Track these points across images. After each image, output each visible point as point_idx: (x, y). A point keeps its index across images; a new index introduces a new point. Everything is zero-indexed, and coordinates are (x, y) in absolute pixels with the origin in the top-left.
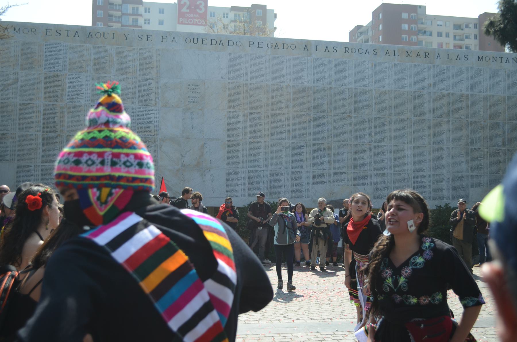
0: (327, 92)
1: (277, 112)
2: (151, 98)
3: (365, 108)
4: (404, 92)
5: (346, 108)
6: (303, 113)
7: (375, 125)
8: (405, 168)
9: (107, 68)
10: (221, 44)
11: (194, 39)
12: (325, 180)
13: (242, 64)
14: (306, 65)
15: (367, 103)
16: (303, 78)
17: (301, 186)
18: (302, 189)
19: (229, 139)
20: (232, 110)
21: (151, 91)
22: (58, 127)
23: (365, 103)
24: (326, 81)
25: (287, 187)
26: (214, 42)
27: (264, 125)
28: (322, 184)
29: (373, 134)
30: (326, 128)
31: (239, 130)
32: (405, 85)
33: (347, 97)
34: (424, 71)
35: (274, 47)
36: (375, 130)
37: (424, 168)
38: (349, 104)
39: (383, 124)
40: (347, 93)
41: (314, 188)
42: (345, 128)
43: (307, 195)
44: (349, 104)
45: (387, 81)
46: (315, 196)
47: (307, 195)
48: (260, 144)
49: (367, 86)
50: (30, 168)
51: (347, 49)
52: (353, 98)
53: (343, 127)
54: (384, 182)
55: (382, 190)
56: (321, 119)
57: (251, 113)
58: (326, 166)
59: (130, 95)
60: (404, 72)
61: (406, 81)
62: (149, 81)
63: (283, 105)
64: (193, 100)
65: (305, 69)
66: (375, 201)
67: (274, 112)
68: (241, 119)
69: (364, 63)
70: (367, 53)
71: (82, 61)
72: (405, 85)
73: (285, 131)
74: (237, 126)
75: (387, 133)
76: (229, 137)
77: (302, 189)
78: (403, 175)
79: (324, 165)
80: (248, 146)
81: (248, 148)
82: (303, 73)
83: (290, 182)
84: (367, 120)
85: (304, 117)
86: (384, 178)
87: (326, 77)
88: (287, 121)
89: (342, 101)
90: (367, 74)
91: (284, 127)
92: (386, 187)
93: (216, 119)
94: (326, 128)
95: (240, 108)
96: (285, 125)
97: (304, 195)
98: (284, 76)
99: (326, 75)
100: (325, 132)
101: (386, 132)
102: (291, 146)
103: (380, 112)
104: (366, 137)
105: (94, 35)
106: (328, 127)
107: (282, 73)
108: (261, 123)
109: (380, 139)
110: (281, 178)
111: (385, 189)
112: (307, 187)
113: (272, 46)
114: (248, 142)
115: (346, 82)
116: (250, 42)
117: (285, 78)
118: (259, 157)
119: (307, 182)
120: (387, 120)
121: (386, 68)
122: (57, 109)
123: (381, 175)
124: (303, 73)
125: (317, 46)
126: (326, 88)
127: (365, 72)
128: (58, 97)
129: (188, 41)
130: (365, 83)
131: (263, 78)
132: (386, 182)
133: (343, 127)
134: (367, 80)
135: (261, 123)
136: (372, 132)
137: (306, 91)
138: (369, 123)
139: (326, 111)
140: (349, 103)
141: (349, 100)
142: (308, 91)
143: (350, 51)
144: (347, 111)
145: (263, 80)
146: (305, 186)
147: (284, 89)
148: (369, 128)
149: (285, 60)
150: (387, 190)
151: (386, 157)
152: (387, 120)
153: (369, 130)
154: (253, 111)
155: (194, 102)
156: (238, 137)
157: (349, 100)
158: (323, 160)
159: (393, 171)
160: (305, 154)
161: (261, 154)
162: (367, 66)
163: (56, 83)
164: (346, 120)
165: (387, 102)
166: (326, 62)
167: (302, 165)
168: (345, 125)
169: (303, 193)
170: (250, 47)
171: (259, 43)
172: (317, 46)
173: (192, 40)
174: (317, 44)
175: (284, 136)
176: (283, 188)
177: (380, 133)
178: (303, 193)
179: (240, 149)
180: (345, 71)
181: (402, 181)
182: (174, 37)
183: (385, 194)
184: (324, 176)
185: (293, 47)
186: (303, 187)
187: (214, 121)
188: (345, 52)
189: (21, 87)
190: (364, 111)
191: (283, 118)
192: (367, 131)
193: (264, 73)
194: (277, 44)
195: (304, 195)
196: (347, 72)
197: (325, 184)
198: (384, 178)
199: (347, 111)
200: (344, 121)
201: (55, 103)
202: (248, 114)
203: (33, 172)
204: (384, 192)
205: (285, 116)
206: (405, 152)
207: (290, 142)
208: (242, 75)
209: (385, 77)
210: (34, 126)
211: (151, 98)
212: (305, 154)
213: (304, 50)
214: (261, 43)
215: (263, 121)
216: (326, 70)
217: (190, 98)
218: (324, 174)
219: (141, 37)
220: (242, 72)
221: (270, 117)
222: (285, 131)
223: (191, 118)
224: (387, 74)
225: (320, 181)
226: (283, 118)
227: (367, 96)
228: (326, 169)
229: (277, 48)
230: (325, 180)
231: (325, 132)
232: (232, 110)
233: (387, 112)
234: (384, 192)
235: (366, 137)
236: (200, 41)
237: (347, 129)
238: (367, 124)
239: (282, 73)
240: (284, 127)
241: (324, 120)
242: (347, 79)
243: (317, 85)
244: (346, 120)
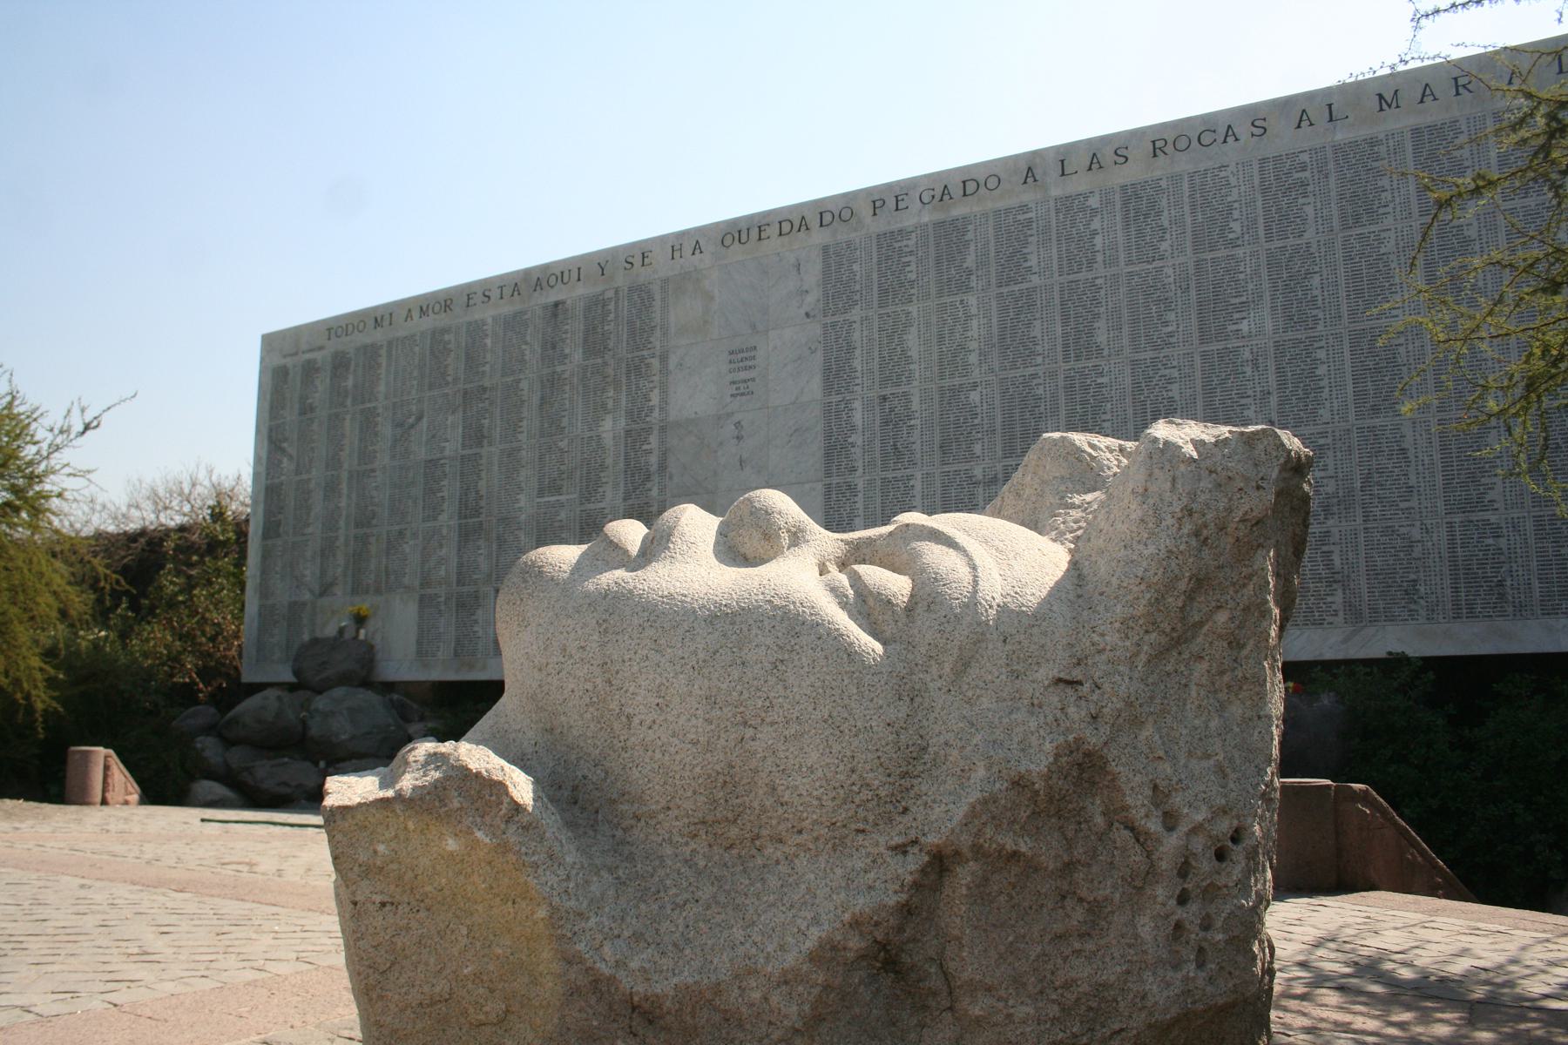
0: (1103, 292)
1: (957, 381)
2: (651, 404)
3: (1236, 316)
4: (1383, 235)
5: (1170, 329)
6: (1031, 370)
7: (1279, 370)
8: (1406, 505)
9: (567, 351)
10: (803, 228)
11: (740, 232)
13: (856, 267)
14: (1034, 225)
15: (1244, 299)
16: (1028, 264)
19: (828, 481)
20: (835, 398)
21: (651, 385)
22: (483, 503)
23: (1237, 300)
24: (1100, 258)
26: (786, 227)
27: (919, 427)
29: (1274, 400)
30: (1109, 405)
31: (853, 450)
32: (1381, 211)
33: (1172, 294)
34: (1457, 142)
35: (938, 197)
36: (1282, 385)
37: (1491, 495)
38: (1180, 315)
39: (1308, 360)
40: (1171, 279)
42: (1170, 394)
44: (1180, 315)
45: (1309, 210)
48: (912, 483)
49: (1239, 242)
50: (439, 600)
51: (1158, 144)
52: (1193, 293)
53: (1164, 393)
54: (1329, 565)
55: (1322, 593)
56: (1089, 381)
57: (884, 398)
59: (610, 404)
60: (1375, 164)
61: (1384, 195)
62: (646, 361)
63: (973, 358)
64: (742, 391)
65: (1030, 239)
66: (1298, 633)
67: (947, 383)
68: (858, 418)
69: (1223, 174)
70: (1230, 139)
71: (524, 347)
72: (1381, 211)
73: (980, 435)
74: (850, 440)
75: (1327, 389)
76: (828, 474)
78: (1403, 530)
80: (879, 493)
81: (879, 500)
82: (1025, 251)
84: (1247, 355)
85: (1035, 382)
86: (1325, 548)
87: (1099, 247)
88: (985, 404)
89: (1154, 311)
90: (1236, 205)
91: (976, 421)
92: (1335, 582)
93: (795, 431)
94: (1109, 405)
95: (856, 388)
96: (979, 417)
98: (970, 273)
99: (1098, 240)
100: (1104, 417)
101: (1322, 384)
103: (1295, 320)
104: (1246, 413)
105: (544, 284)
106: (1114, 402)
107: (965, 265)
108: (912, 422)
109: (1301, 413)
111: (1335, 586)
113: (933, 197)
114: (879, 483)
115: (1164, 246)
116: (874, 202)
117: (973, 278)
120: (1323, 343)
121: (1304, 169)
122: (481, 462)
123: (1313, 540)
124: (1025, 251)
125: (1062, 161)
126: (1098, 282)
127: (1229, 199)
128: (483, 436)
129: (728, 241)
130: (1231, 236)
131: (912, 291)
132: (1337, 561)
133: (1164, 393)
134: (1236, 226)
135: (912, 422)
136: (1269, 393)
137: (1039, 303)
138: (1256, 366)
139: (1106, 352)
140: (1179, 311)
141: (1180, 303)
142: (1044, 302)
143: (1169, 149)
144: (1173, 340)
145: (914, 298)
147: (974, 311)
148: (1256, 381)
149: (970, 227)
150: (1340, 592)
151: (1331, 472)
152: (1323, 343)
153: (1258, 389)
154: (888, 391)
155: (743, 394)
156: (853, 470)
157: (1180, 303)
159: (1360, 520)
162: (1233, 181)
163: (480, 405)
164: (1174, 367)
165: (1316, 280)
166: (1094, 202)
168: (1170, 387)
170: (875, 214)
171: (900, 198)
172: (1062, 161)
173: (737, 236)
174: (1063, 158)
175: (977, 449)
177: (1300, 392)
179: (857, 505)
180: (1159, 213)
181: (1402, 554)
182: (697, 242)
183: (1334, 607)
185: (992, 183)
187: (791, 435)
188: (1155, 156)
189: (428, 428)
190: (1235, 327)
191: (974, 396)
192: (1250, 393)
193: (913, 276)
194: (946, 187)
196: (1166, 213)
198: (1325, 548)
199: (1173, 340)
200: (1167, 372)
201: (478, 450)
202: (877, 401)
203: (443, 608)
204: (1329, 599)
205: (979, 389)
206: (1405, 445)
207: (999, 467)
208: (857, 297)
209: (1301, 201)
210: (445, 506)
211: (651, 404)
213: (1025, 182)
214: (904, 196)
215: (917, 415)
216: (1096, 225)
217: (735, 386)
219: (630, 260)
220: (858, 287)
221: (937, 397)
222: (980, 435)
223: (738, 438)
224: (1310, 188)
226: (974, 396)
227: (1242, 276)
229: (946, 197)
231: (1104, 417)
232: (835, 398)
233: (1321, 315)
234: (1329, 599)
235: (1246, 413)
236: (754, 233)
237: (1177, 398)
238: (1248, 370)
239: (965, 265)
240: (976, 421)
241: (1099, 381)
242: (1167, 236)
243: (1071, 277)
244: (1174, 367)
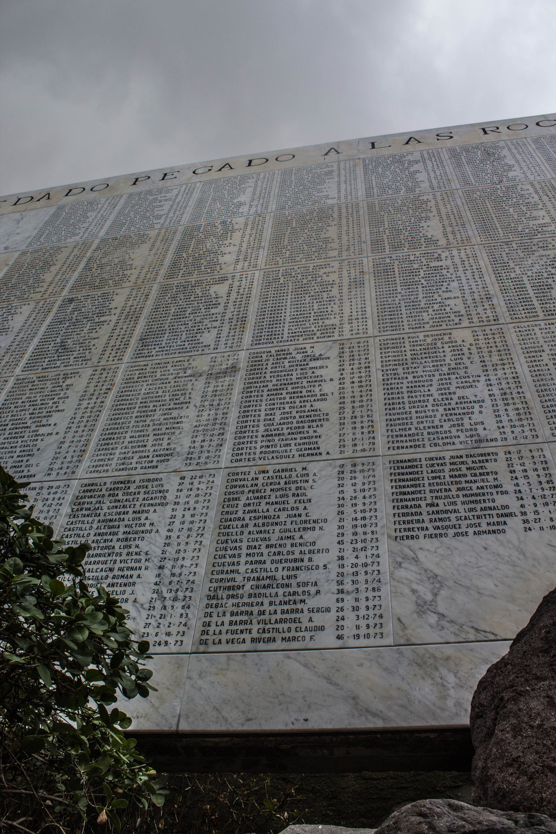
12: (501, 500)
17: (297, 556)
18: (303, 576)
25: (177, 571)
28: (484, 527)
41: (416, 560)
43: (350, 616)
46: (433, 619)
47: (350, 616)
58: (491, 422)
77: (303, 576)
79: (476, 417)
83: (208, 540)
97: (319, 619)
102: (242, 365)
110: (144, 516)
112: (350, 560)
118: (42, 430)
119: (348, 524)
146: (334, 553)
158: (459, 398)
160: (327, 388)
161: (56, 418)
167: (311, 433)
169: (312, 603)
176: (150, 576)
178: (312, 603)
184: (490, 478)
186: (319, 559)
195: (319, 619)
197: (515, 523)
212: (327, 388)
218: (486, 464)
225: (460, 507)
228: (497, 435)
230: (501, 500)
